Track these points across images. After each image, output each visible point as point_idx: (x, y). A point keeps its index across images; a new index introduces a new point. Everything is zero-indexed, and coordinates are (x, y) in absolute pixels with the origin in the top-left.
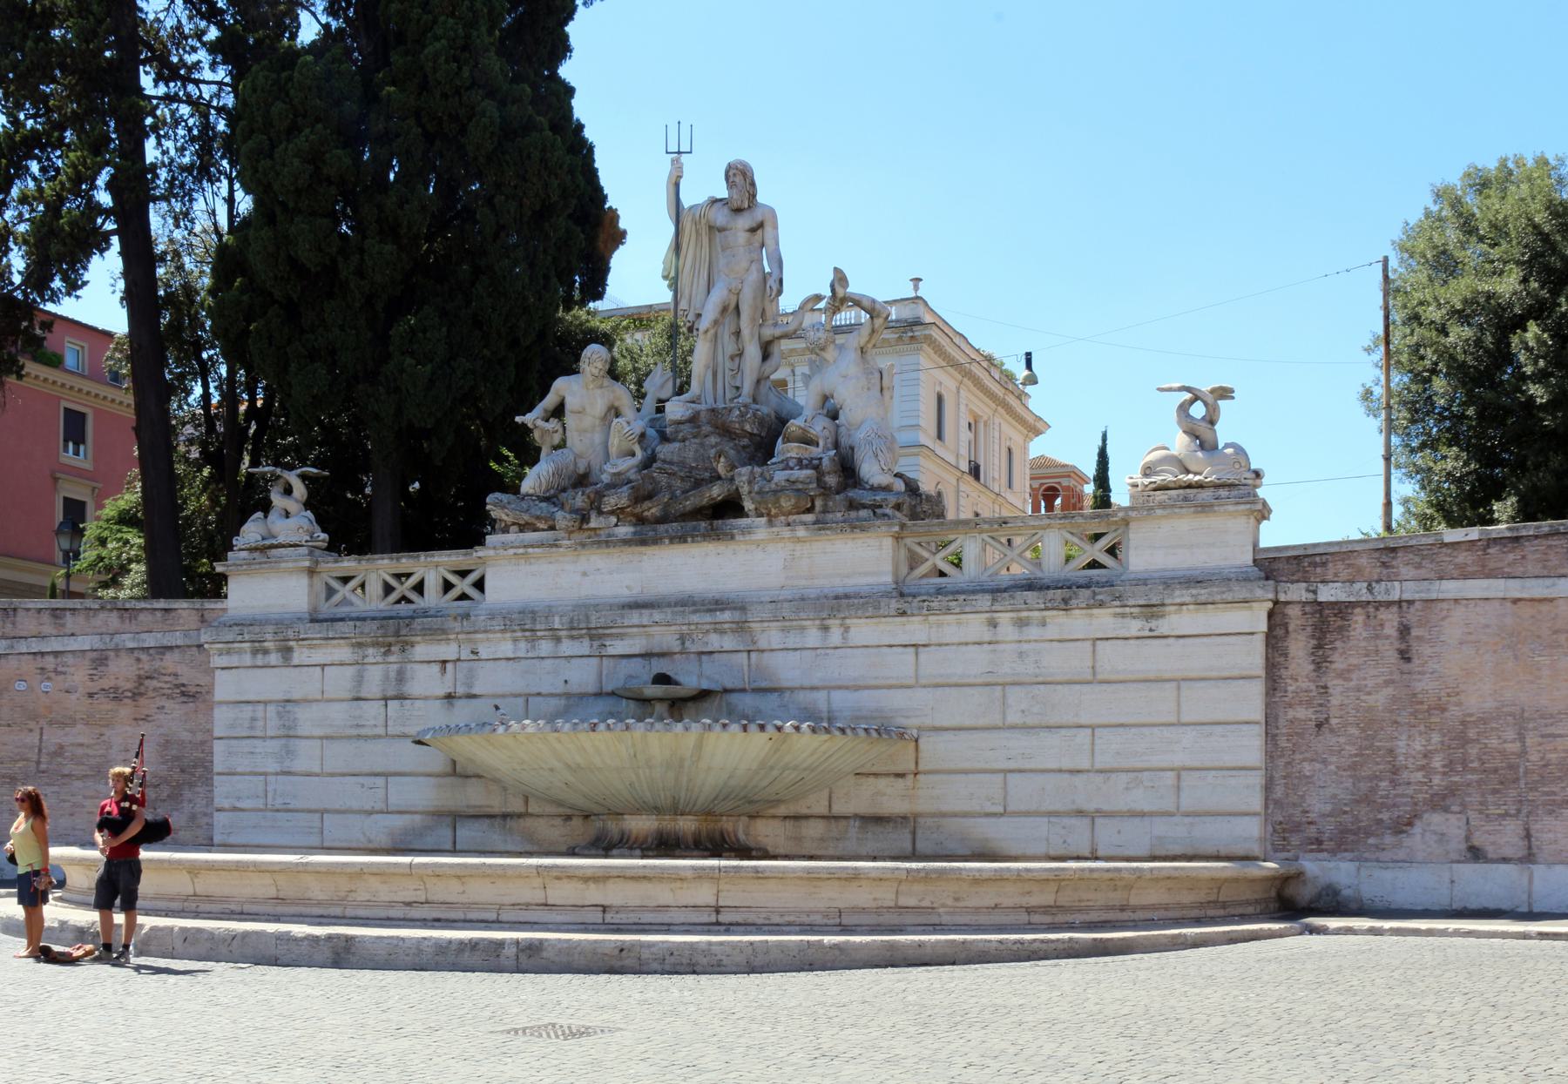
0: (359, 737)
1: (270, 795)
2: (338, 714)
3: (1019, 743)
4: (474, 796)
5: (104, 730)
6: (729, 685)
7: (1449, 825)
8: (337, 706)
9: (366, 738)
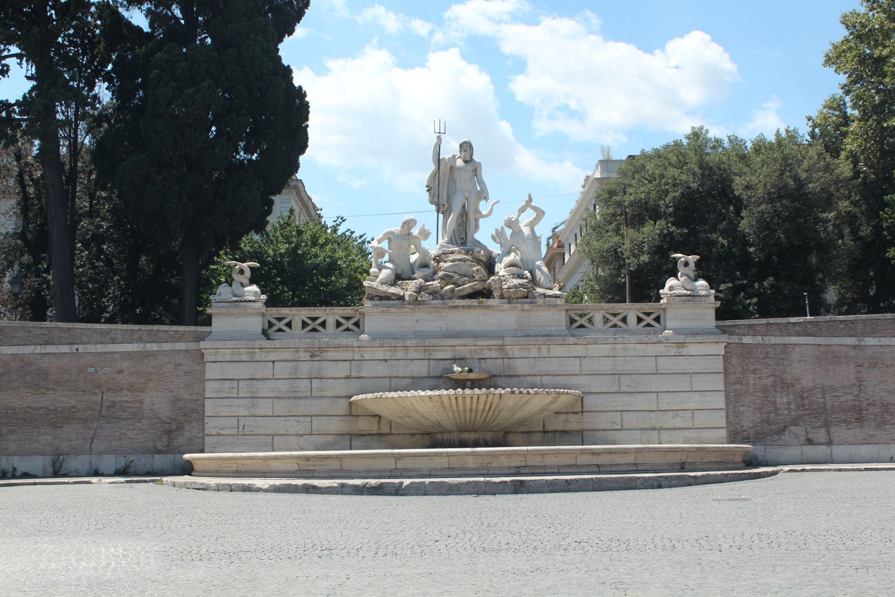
0: (295, 398)
1: (241, 427)
3: (626, 399)
4: (363, 425)
5: (140, 394)
6: (495, 373)
7: (800, 430)
8: (282, 381)
9: (300, 398)
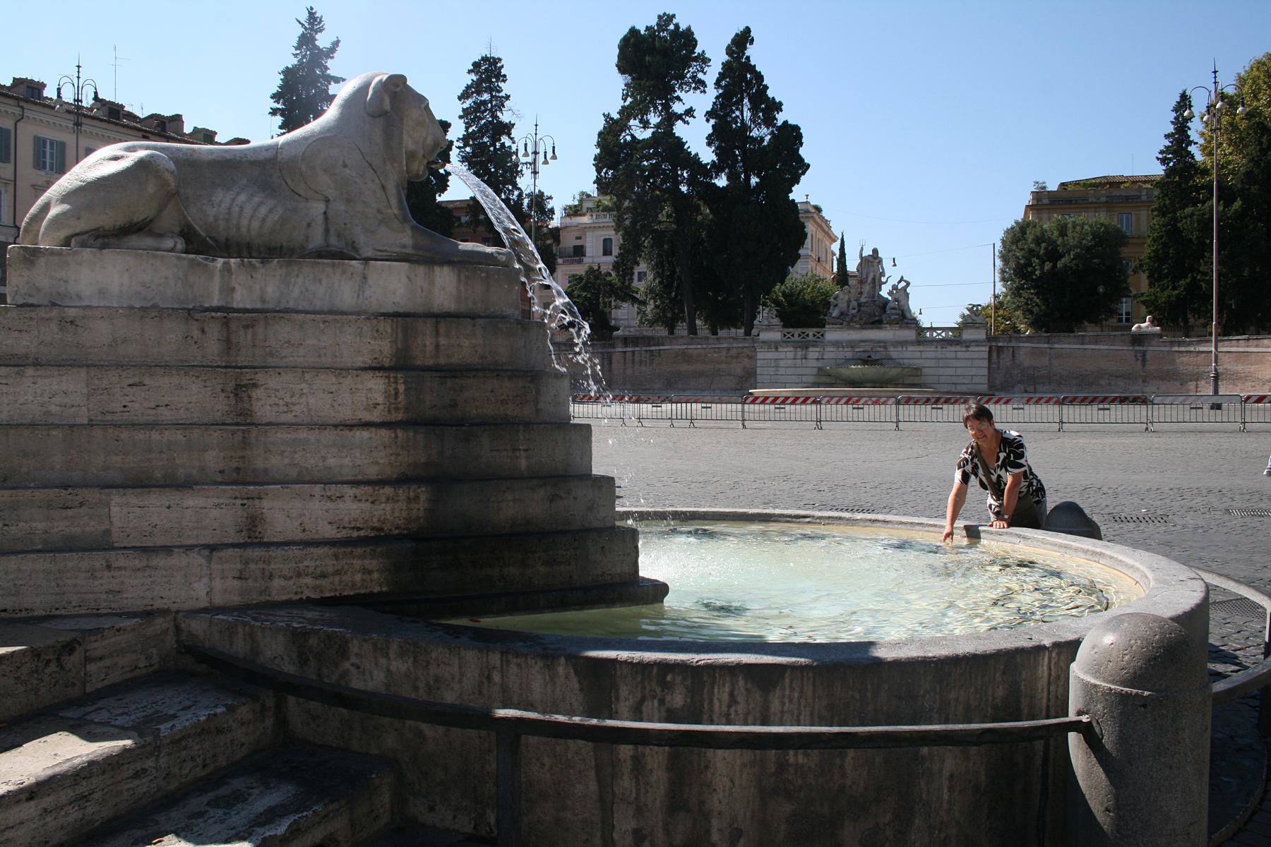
2: (790, 362)
